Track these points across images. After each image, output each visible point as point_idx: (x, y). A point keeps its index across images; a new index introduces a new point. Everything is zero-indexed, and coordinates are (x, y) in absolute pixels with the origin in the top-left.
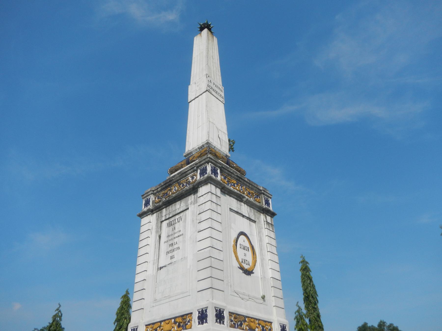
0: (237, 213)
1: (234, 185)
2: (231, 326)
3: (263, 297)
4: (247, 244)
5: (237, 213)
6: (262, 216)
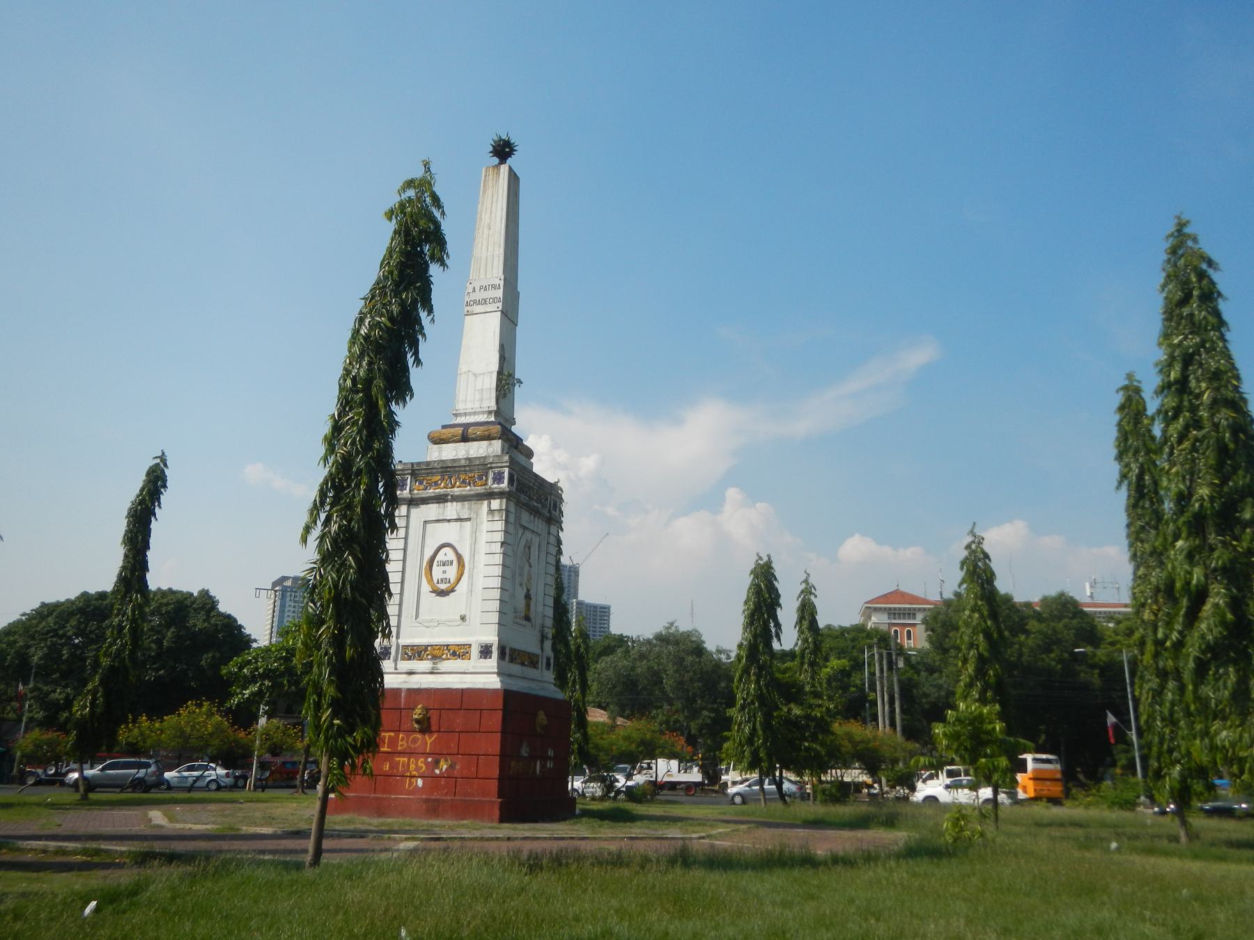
0: (438, 521)
1: (436, 483)
2: (403, 659)
3: (463, 618)
4: (451, 555)
5: (438, 521)
6: (486, 502)
